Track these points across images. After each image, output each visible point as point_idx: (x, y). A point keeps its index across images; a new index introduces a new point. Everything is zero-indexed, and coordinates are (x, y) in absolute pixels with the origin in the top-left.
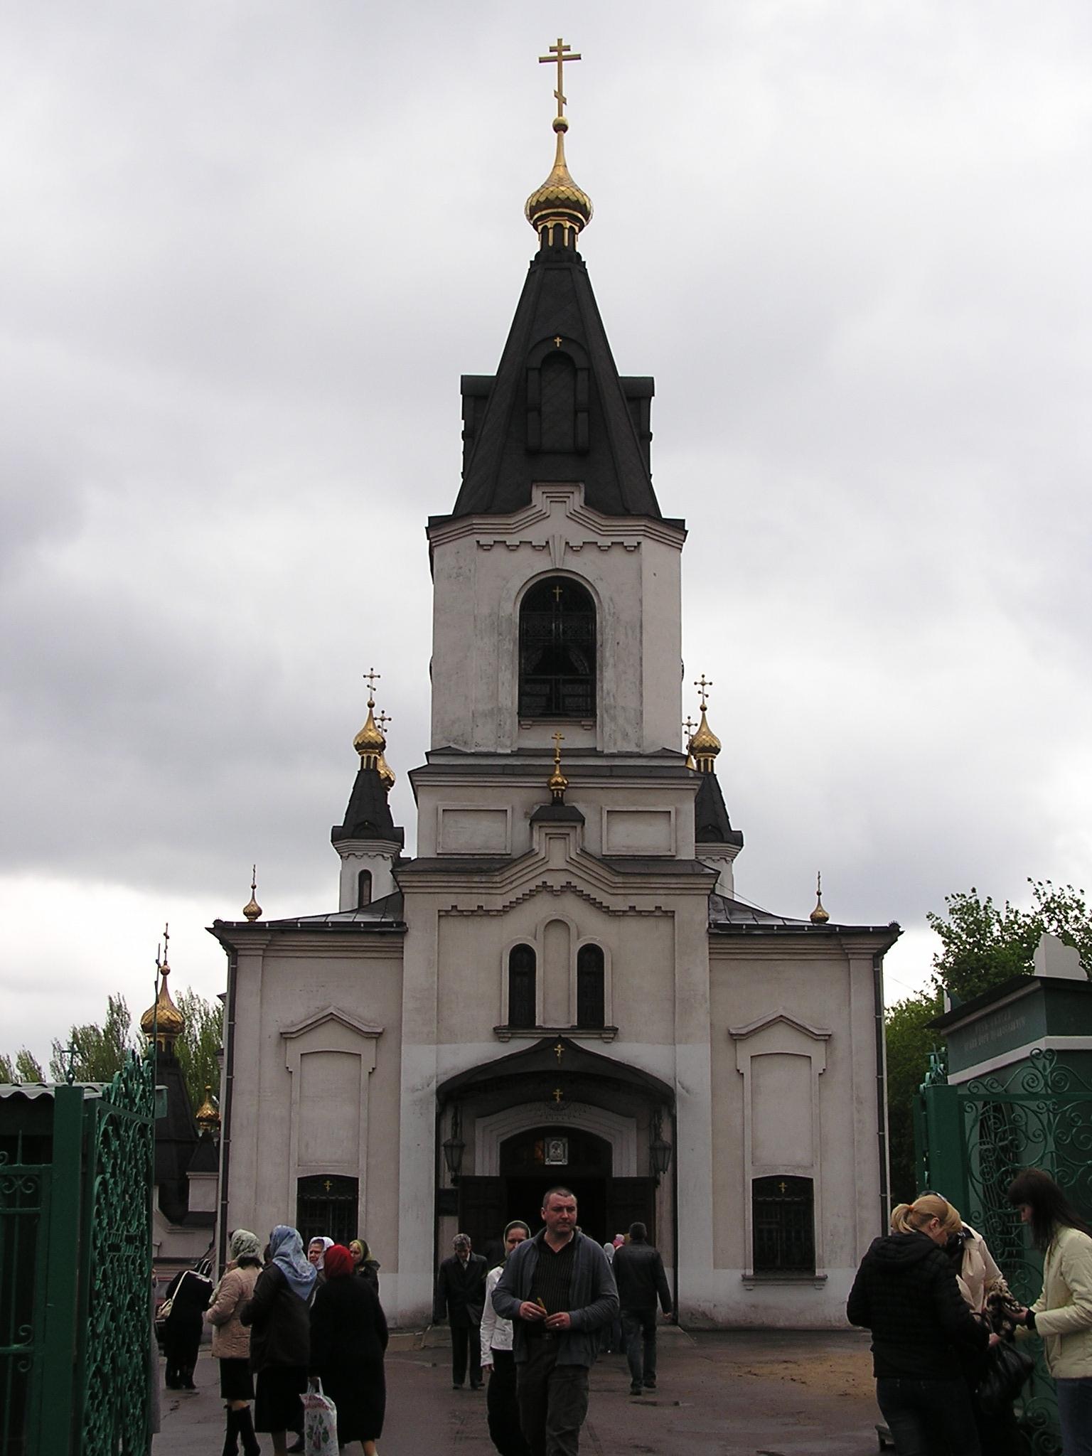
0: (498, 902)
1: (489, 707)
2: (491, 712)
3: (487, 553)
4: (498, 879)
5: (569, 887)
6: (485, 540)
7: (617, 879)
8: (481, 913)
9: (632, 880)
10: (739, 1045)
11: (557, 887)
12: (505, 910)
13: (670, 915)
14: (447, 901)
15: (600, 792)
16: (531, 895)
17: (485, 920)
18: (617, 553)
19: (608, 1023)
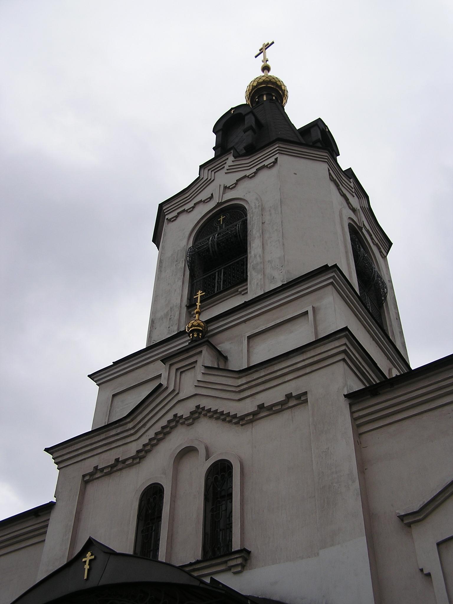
0: (133, 449)
1: (166, 311)
2: (166, 315)
3: (174, 223)
4: (130, 425)
5: (199, 413)
6: (169, 216)
7: (240, 382)
8: (117, 466)
9: (256, 376)
10: (416, 531)
11: (187, 415)
12: (141, 456)
13: (301, 399)
14: (88, 466)
15: (243, 326)
16: (165, 433)
17: (124, 472)
18: (264, 175)
19: (236, 546)
